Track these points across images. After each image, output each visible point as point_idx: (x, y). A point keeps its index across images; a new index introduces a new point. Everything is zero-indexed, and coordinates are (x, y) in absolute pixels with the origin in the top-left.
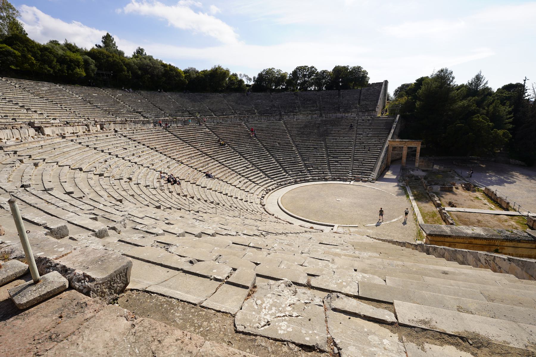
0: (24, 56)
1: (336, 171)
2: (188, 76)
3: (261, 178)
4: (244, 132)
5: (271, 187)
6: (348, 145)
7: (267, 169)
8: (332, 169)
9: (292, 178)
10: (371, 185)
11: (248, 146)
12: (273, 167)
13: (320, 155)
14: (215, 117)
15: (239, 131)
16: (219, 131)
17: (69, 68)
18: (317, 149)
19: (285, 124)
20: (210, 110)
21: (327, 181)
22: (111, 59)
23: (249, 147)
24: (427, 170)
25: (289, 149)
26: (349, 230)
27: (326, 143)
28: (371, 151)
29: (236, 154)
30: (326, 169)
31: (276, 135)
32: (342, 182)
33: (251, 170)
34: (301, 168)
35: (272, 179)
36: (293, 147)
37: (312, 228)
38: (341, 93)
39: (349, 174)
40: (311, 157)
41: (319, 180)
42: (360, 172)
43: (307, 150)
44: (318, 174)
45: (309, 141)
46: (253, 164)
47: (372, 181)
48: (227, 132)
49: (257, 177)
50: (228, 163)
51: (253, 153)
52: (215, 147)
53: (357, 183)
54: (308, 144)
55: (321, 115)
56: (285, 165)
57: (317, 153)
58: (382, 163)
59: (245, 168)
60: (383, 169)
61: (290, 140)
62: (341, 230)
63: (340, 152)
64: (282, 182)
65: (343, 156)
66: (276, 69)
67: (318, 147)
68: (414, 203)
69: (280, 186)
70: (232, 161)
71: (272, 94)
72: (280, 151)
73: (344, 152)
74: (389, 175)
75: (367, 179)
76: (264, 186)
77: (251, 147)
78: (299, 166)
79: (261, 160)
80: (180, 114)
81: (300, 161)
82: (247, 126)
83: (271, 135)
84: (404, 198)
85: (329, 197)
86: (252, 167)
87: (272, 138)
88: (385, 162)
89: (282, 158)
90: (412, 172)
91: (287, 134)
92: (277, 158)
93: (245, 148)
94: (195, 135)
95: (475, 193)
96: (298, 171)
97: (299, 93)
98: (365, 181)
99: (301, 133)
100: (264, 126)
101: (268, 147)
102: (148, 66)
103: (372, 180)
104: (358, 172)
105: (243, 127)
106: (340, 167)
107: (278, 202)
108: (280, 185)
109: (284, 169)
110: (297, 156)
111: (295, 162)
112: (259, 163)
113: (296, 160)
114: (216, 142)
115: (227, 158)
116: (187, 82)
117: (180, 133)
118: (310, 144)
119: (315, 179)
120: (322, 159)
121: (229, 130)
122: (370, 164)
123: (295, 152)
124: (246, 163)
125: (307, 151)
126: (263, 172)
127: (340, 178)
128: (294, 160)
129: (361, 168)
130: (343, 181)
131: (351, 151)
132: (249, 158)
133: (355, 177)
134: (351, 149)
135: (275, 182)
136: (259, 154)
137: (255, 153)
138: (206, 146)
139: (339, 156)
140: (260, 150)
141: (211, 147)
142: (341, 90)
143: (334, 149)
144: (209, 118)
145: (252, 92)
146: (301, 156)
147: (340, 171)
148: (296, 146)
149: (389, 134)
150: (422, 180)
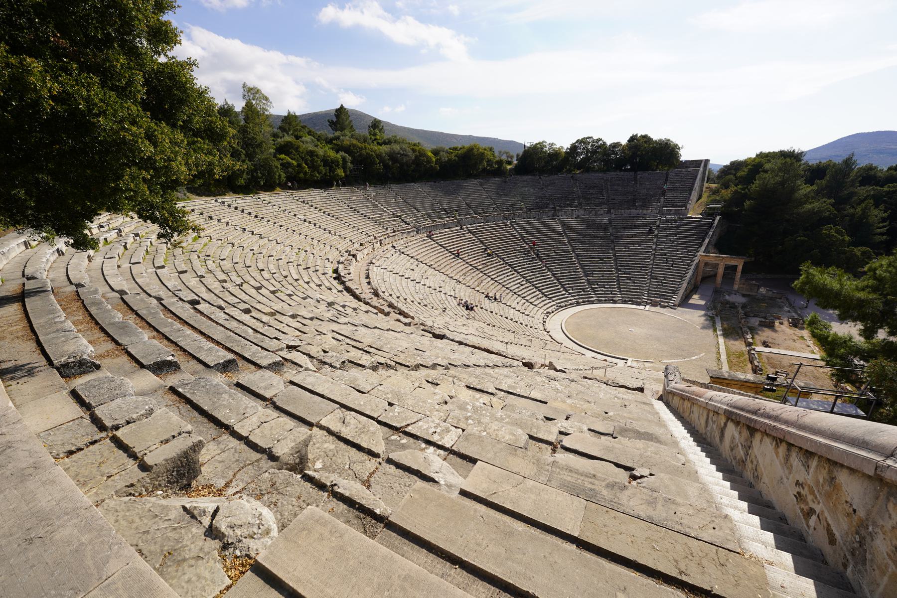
0: (299, 165)
1: (627, 291)
5: (551, 308)
7: (543, 286)
8: (623, 288)
13: (607, 268)
16: (483, 236)
17: (330, 170)
18: (603, 260)
19: (561, 223)
21: (615, 303)
22: (364, 152)
24: (749, 295)
27: (615, 253)
28: (675, 267)
30: (615, 288)
32: (634, 306)
33: (526, 288)
34: (583, 286)
35: (550, 298)
37: (605, 360)
39: (644, 295)
41: (606, 302)
42: (658, 294)
44: (605, 294)
46: (527, 280)
47: (673, 307)
50: (500, 279)
51: (524, 265)
52: (483, 257)
55: (609, 212)
56: (563, 282)
57: (603, 266)
58: (688, 283)
60: (688, 291)
62: (635, 364)
64: (562, 302)
67: (605, 258)
68: (721, 340)
69: (560, 307)
73: (639, 267)
74: (696, 299)
75: (667, 304)
77: (522, 257)
78: (580, 283)
79: (535, 275)
81: (582, 277)
84: (710, 332)
88: (693, 282)
89: (559, 272)
90: (727, 297)
92: (553, 271)
94: (459, 243)
95: (802, 331)
96: (580, 289)
97: (579, 175)
98: (664, 307)
100: (534, 227)
102: (398, 154)
104: (656, 294)
106: (632, 286)
109: (563, 286)
111: (576, 278)
112: (533, 278)
113: (578, 275)
114: (482, 252)
119: (601, 300)
120: (610, 274)
122: (672, 284)
124: (519, 279)
126: (539, 290)
127: (632, 301)
128: (575, 275)
129: (660, 288)
131: (648, 265)
132: (522, 272)
133: (651, 300)
135: (554, 303)
136: (532, 267)
138: (474, 257)
139: (632, 272)
142: (638, 173)
146: (583, 269)
147: (632, 292)
148: (577, 255)
149: (701, 244)
150: (740, 309)
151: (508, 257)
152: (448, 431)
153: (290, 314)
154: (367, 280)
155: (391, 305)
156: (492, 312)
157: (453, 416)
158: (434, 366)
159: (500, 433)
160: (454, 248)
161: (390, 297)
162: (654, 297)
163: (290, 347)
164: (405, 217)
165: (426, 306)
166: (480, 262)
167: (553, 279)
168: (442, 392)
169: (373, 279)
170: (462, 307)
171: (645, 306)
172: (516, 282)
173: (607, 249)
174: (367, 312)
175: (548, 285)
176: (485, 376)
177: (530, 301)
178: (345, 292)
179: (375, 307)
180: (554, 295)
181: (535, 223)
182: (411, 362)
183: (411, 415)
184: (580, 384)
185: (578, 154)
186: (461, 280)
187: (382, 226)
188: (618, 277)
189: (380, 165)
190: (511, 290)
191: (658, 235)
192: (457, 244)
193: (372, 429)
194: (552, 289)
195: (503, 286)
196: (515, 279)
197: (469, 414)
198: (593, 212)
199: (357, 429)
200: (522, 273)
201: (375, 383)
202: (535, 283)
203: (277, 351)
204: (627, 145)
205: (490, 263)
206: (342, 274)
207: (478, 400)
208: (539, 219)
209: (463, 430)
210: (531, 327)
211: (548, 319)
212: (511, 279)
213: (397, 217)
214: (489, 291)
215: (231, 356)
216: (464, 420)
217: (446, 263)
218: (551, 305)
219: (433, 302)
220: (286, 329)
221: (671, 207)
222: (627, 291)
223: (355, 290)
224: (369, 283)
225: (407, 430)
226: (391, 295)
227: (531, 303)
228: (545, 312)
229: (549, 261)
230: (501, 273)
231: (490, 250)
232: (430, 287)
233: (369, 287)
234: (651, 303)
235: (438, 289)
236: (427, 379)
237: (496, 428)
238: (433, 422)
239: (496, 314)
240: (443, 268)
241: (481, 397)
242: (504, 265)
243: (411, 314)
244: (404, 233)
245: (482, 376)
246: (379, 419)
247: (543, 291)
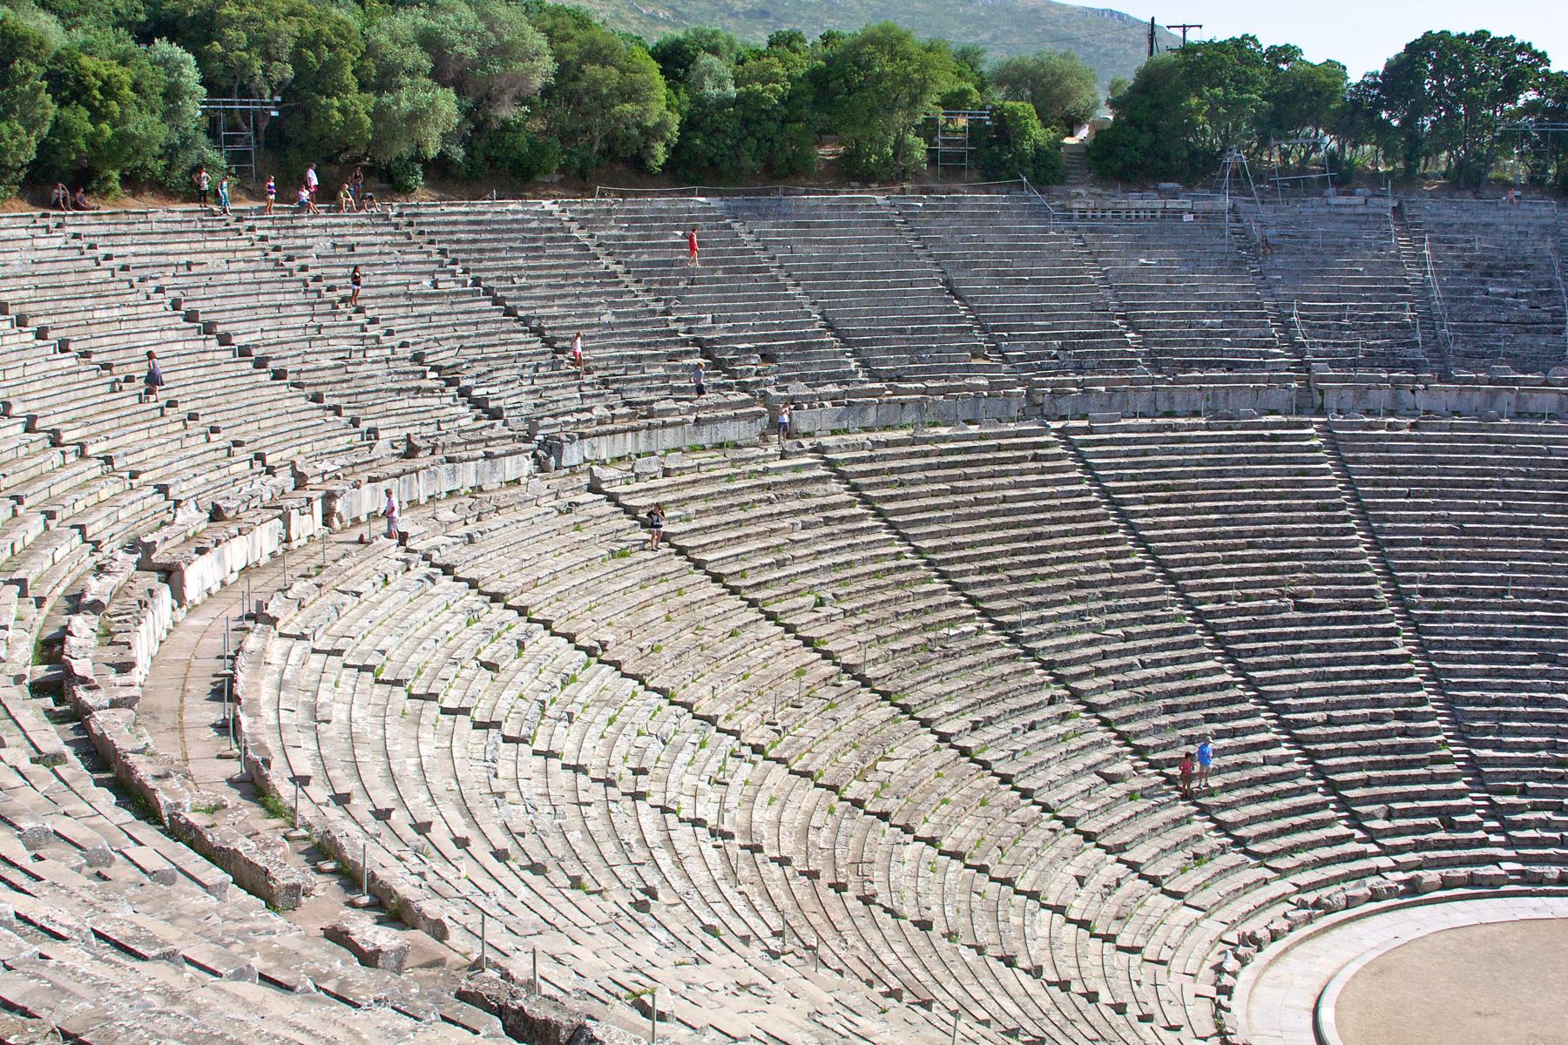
3: (1196, 856)
4: (1066, 507)
9: (1385, 862)
11: (1099, 612)
12: (1266, 780)
16: (905, 497)
20: (830, 327)
25: (1371, 646)
43: (1485, 660)
48: (956, 505)
51: (1131, 667)
54: (1494, 619)
56: (1341, 769)
64: (1326, 883)
76: (1219, 915)
77: (1120, 624)
78: (1433, 779)
79: (1186, 724)
82: (1079, 456)
83: (1240, 535)
87: (1253, 559)
89: (1319, 716)
92: (1287, 709)
93: (1079, 630)
101: (1225, 627)
110: (1422, 701)
111: (1409, 748)
113: (1418, 733)
119: (1541, 880)
121: (969, 491)
123: (1410, 673)
124: (1100, 744)
132: (1115, 705)
140: (1174, 647)
154: (216, 712)
155: (322, 851)
161: (334, 813)
165: (537, 869)
169: (254, 702)
175: (1252, 783)
178: (74, 767)
180: (1285, 841)
194: (1277, 805)
206: (81, 667)
210: (1146, 1018)
211: (1246, 974)
219: (583, 848)
223: (132, 758)
224: (229, 728)
226: (342, 800)
228: (1232, 937)
229: (1267, 651)
232: (578, 769)
233: (228, 745)
235: (627, 783)
243: (432, 908)
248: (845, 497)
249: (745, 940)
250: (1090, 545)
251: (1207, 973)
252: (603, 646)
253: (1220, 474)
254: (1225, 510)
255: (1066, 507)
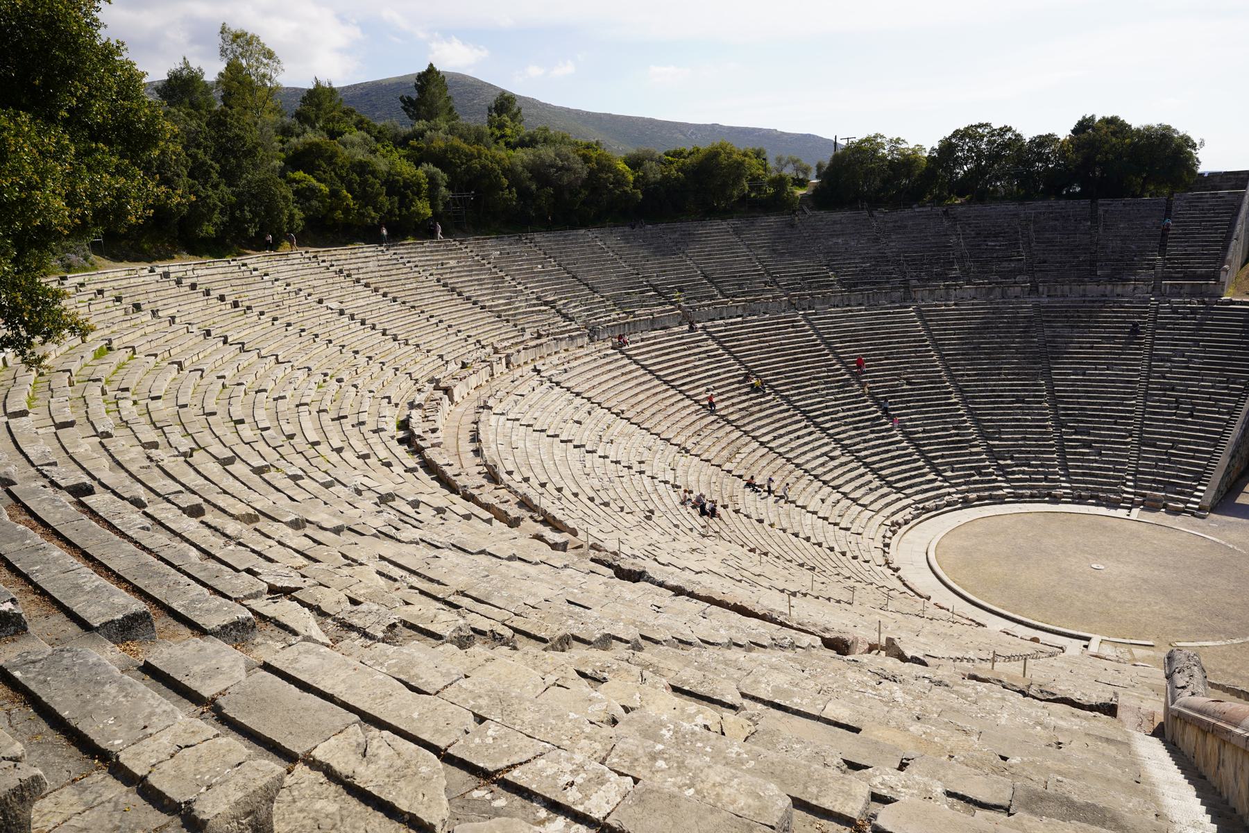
0: (334, 194)
1: (1084, 474)
2: (642, 177)
3: (870, 489)
4: (807, 346)
5: (901, 514)
6: (1124, 393)
7: (882, 461)
8: (1073, 467)
10: (1194, 526)
11: (824, 389)
13: (1033, 420)
14: (722, 303)
15: (792, 343)
16: (740, 346)
18: (1023, 402)
21: (1057, 503)
22: (476, 164)
23: (827, 394)
26: (1132, 654)
28: (1198, 417)
29: (796, 415)
30: (1054, 466)
31: (898, 353)
32: (1102, 510)
33: (842, 465)
34: (977, 461)
35: (899, 490)
36: (951, 393)
37: (1035, 640)
38: (1101, 211)
39: (1124, 485)
40: (1007, 427)
41: (1033, 498)
42: (1160, 482)
44: (1030, 480)
45: (999, 374)
46: (844, 447)
47: (1200, 512)
48: (761, 348)
49: (860, 487)
50: (782, 445)
51: (838, 412)
52: (740, 395)
53: (1150, 517)
54: (995, 385)
55: (1034, 290)
56: (931, 451)
57: (1024, 414)
58: (1233, 457)
59: (825, 458)
60: (1234, 476)
61: (940, 371)
62: (1108, 651)
63: (1098, 416)
64: (927, 499)
65: (1108, 429)
66: (888, 137)
67: (1028, 396)
69: (923, 511)
70: (791, 440)
71: (875, 213)
72: (913, 407)
73: (1110, 417)
75: (1181, 506)
77: (833, 394)
78: (971, 454)
80: (636, 298)
81: (975, 440)
82: (811, 324)
83: (882, 354)
85: (1069, 556)
86: (843, 454)
87: (888, 364)
89: (920, 429)
91: (930, 351)
92: (905, 426)
93: (815, 397)
94: (686, 363)
98: (1177, 512)
99: (974, 349)
100: (860, 325)
101: (878, 393)
102: (552, 166)
103: (1199, 510)
104: (1154, 481)
105: (801, 331)
106: (1096, 461)
107: (931, 560)
108: (923, 508)
109: (929, 461)
110: (965, 421)
111: (960, 441)
112: (858, 443)
113: (964, 435)
114: (739, 382)
115: (776, 429)
116: (641, 196)
117: (652, 358)
118: (1003, 385)
119: (1022, 496)
120: (1040, 433)
121: (766, 342)
122: (1193, 458)
123: (959, 409)
124: (827, 444)
125: (994, 409)
126: (872, 470)
127: (1097, 497)
128: (957, 435)
129: (1164, 468)
130: (1107, 506)
131: (1132, 412)
132: (832, 428)
133: (1144, 495)
134: (1133, 405)
135: (909, 501)
136: (855, 416)
137: (844, 411)
139: (1094, 428)
141: (732, 397)
142: (1100, 201)
143: (1079, 403)
144: (709, 305)
145: (811, 209)
146: (977, 422)
147: (1096, 476)
148: (960, 390)
151: (799, 394)
152: (600, 781)
153: (289, 519)
154: (473, 446)
155: (525, 503)
156: (761, 521)
157: (623, 750)
158: (606, 641)
159: (727, 790)
160: (673, 373)
161: (525, 485)
162: (1150, 488)
163: (276, 592)
164: (565, 305)
165: (606, 504)
166: (733, 405)
167: (905, 444)
168: (608, 698)
169: (487, 442)
170: (690, 509)
171: (1130, 509)
172: (818, 452)
173: (1033, 374)
174: (467, 517)
175: (893, 458)
176: (720, 667)
177: (851, 496)
178: (421, 473)
179: (487, 507)
180: (908, 482)
181: (861, 316)
182: (552, 630)
183: (521, 744)
184: (956, 692)
185: (959, 162)
186: (689, 445)
187: (511, 324)
188: (1061, 440)
189: (510, 192)
190: (806, 471)
191: (1152, 344)
192: (681, 364)
193: (424, 769)
194: (904, 467)
195: (788, 460)
196: (817, 444)
197: (660, 747)
198: (998, 291)
199: (391, 770)
200: (831, 432)
201: (453, 672)
202: (863, 453)
203: (246, 597)
204: (1071, 140)
205: (757, 408)
206: (418, 432)
207: (691, 717)
208: (871, 307)
209: (636, 781)
210: (855, 558)
211: (895, 538)
212: (806, 444)
213: (546, 303)
214: (755, 471)
215: (138, 606)
216: (645, 759)
217: (656, 408)
218: (902, 507)
220: (275, 552)
221: (1183, 278)
222: (1084, 474)
223: (445, 468)
224: (477, 452)
225: (508, 776)
226: (526, 480)
227: (854, 500)
228: (888, 522)
230: (782, 431)
231: (757, 377)
232: (617, 462)
233: (478, 460)
234: (1142, 503)
235: (636, 467)
236: (582, 669)
237: (718, 779)
238: (569, 760)
239: (772, 525)
240: (648, 419)
241: (699, 712)
242: (791, 412)
243: (571, 524)
244: (561, 339)
245: (713, 665)
246: (450, 751)
247: (883, 472)
248: (715, 346)
249: (691, 530)
250: (818, 362)
251: (879, 538)
252: (623, 412)
253: (872, 329)
254: (875, 344)
255: (807, 346)
